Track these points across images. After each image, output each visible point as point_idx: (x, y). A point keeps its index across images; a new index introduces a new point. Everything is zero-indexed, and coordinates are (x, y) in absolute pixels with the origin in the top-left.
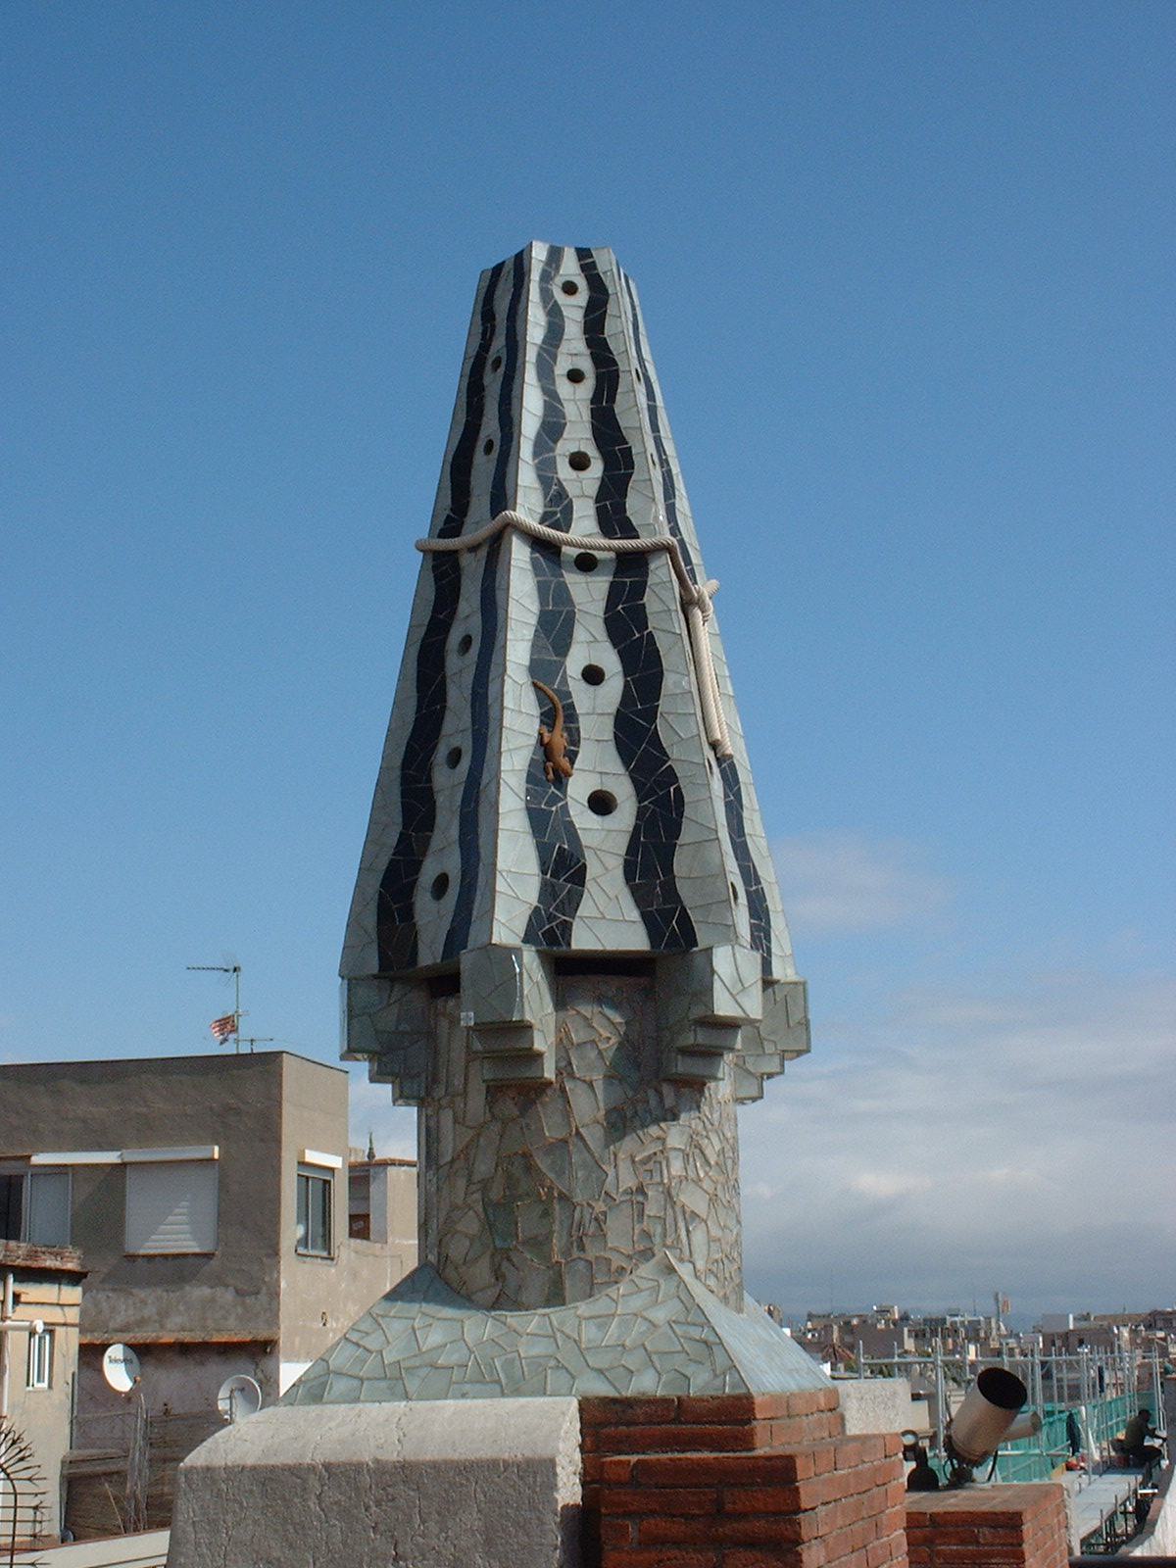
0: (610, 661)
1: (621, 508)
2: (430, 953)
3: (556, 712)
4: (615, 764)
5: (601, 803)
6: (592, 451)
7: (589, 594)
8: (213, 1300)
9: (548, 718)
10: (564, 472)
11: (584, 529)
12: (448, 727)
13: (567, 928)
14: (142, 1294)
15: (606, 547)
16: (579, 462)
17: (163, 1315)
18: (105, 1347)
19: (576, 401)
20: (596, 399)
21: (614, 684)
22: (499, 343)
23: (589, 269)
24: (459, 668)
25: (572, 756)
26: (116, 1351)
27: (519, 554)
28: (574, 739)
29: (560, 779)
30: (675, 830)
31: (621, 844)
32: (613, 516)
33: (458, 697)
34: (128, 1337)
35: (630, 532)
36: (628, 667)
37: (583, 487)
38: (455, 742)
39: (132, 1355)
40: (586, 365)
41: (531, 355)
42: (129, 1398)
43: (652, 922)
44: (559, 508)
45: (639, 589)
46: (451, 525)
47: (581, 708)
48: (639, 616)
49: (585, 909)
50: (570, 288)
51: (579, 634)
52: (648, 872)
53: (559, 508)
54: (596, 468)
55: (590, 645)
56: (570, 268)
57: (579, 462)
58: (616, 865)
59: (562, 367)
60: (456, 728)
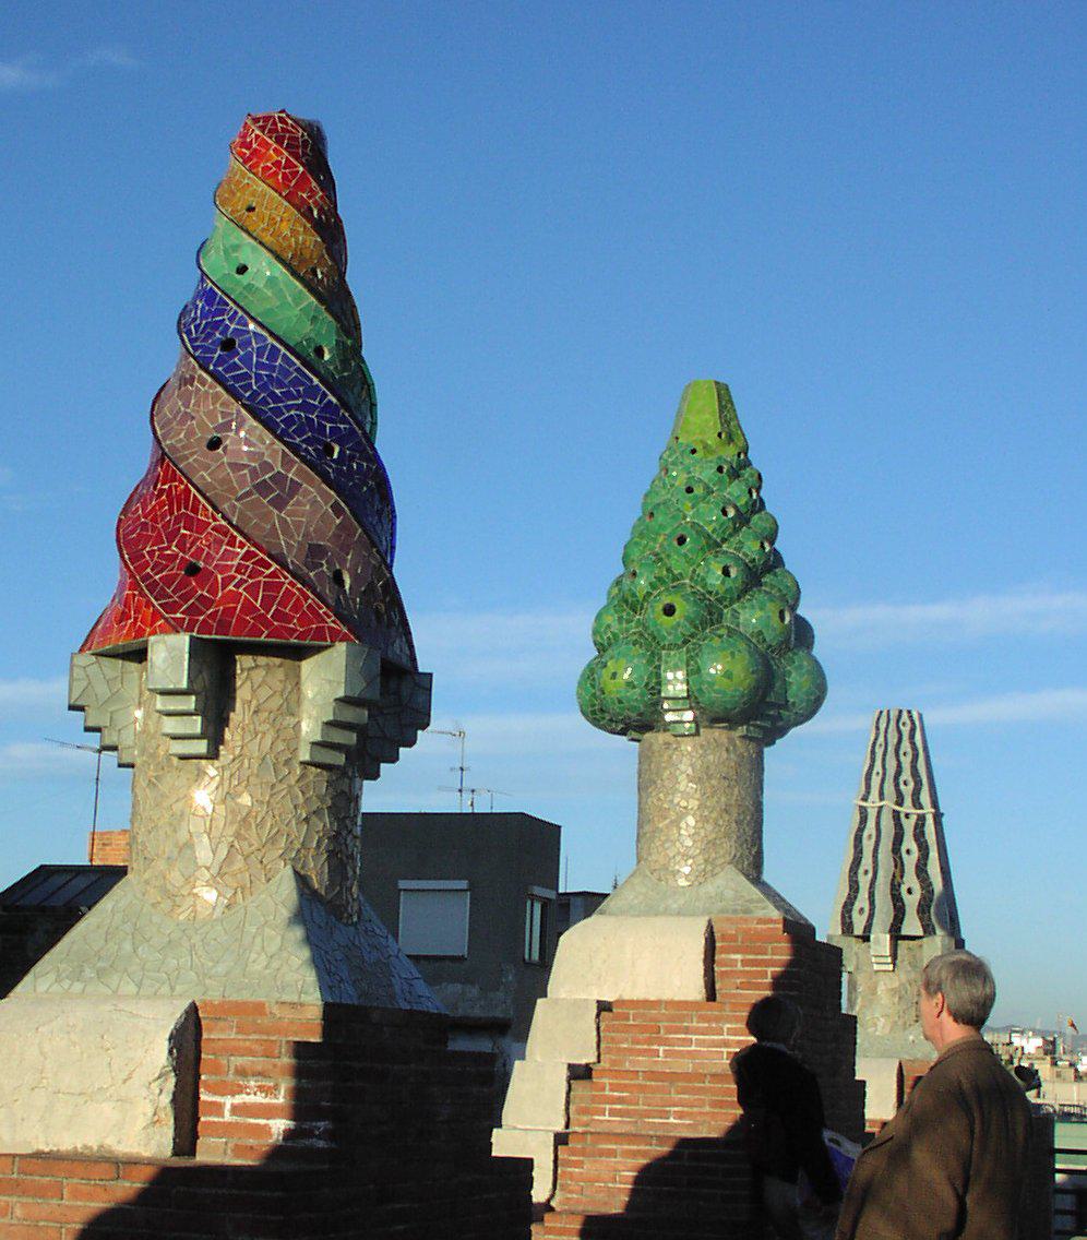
0: (914, 847)
2: (858, 930)
9: (896, 866)
10: (902, 787)
12: (863, 861)
20: (912, 762)
22: (881, 739)
23: (911, 717)
35: (921, 808)
38: (866, 868)
40: (909, 750)
41: (891, 749)
46: (865, 799)
47: (905, 863)
57: (905, 783)
59: (901, 752)
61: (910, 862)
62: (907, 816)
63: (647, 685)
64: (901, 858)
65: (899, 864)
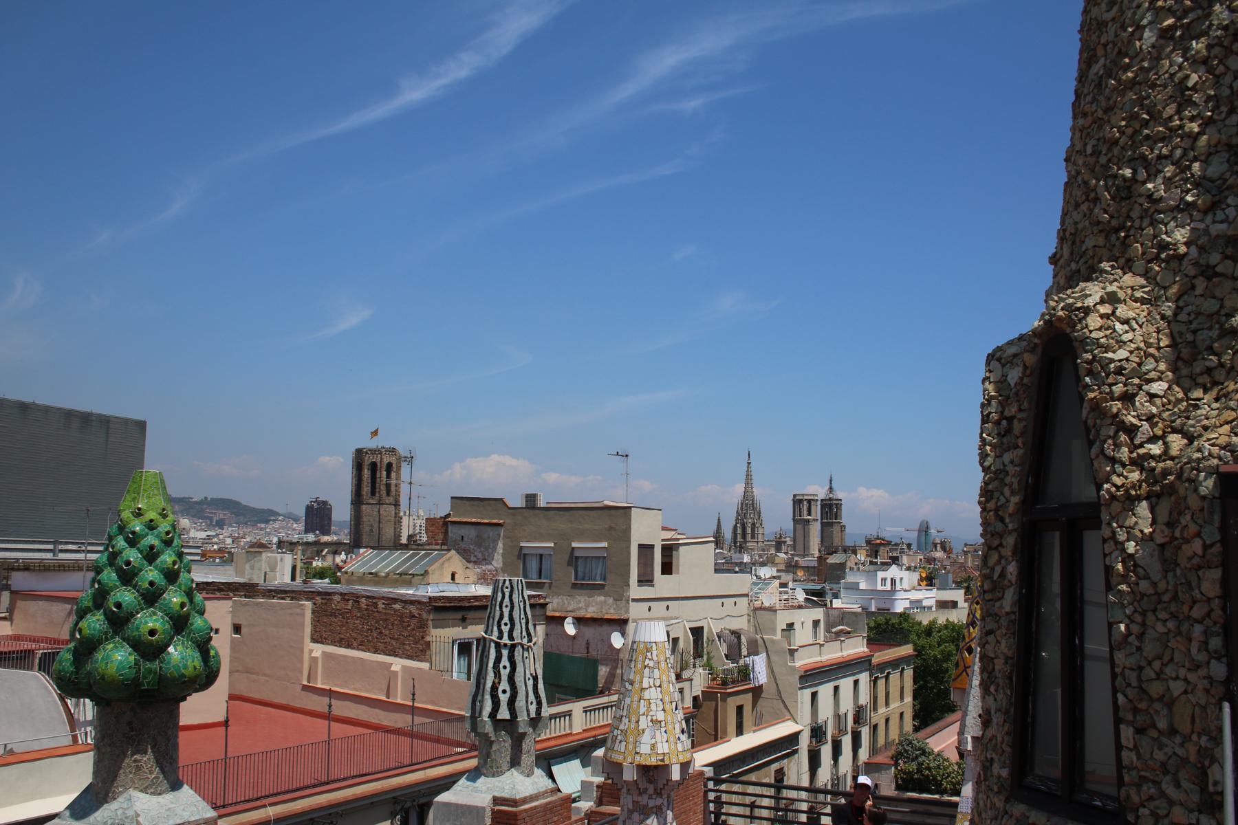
0: (508, 665)
1: (512, 634)
3: (497, 674)
4: (507, 685)
5: (504, 692)
6: (508, 622)
7: (505, 652)
8: (605, 602)
9: (495, 677)
10: (503, 627)
11: (505, 640)
13: (496, 716)
14: (579, 598)
15: (508, 642)
16: (506, 624)
17: (587, 606)
18: (566, 617)
19: (506, 611)
21: (508, 670)
23: (511, 584)
24: (485, 660)
25: (499, 683)
26: (569, 620)
27: (493, 645)
28: (500, 679)
29: (497, 688)
30: (516, 697)
31: (507, 700)
32: (511, 637)
33: (484, 667)
34: (573, 614)
36: (511, 666)
37: (506, 629)
39: (575, 621)
40: (509, 604)
42: (574, 637)
43: (511, 714)
44: (501, 636)
45: (514, 651)
48: (513, 656)
49: (500, 711)
50: (507, 588)
51: (503, 660)
52: (511, 705)
53: (501, 636)
54: (509, 626)
55: (505, 661)
56: (507, 583)
58: (506, 703)
60: (484, 672)
61: (505, 673)
62: (505, 645)
63: (70, 679)
64: (499, 671)
65: (497, 674)
